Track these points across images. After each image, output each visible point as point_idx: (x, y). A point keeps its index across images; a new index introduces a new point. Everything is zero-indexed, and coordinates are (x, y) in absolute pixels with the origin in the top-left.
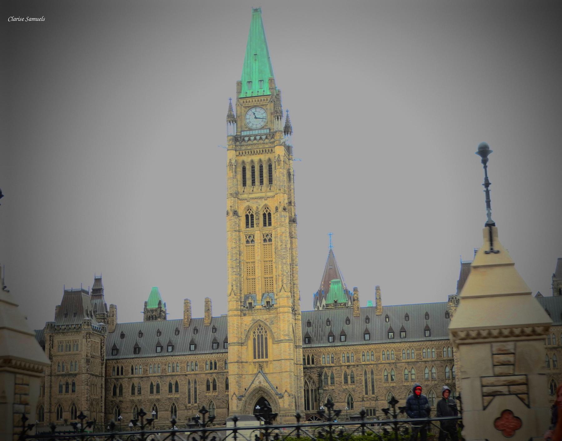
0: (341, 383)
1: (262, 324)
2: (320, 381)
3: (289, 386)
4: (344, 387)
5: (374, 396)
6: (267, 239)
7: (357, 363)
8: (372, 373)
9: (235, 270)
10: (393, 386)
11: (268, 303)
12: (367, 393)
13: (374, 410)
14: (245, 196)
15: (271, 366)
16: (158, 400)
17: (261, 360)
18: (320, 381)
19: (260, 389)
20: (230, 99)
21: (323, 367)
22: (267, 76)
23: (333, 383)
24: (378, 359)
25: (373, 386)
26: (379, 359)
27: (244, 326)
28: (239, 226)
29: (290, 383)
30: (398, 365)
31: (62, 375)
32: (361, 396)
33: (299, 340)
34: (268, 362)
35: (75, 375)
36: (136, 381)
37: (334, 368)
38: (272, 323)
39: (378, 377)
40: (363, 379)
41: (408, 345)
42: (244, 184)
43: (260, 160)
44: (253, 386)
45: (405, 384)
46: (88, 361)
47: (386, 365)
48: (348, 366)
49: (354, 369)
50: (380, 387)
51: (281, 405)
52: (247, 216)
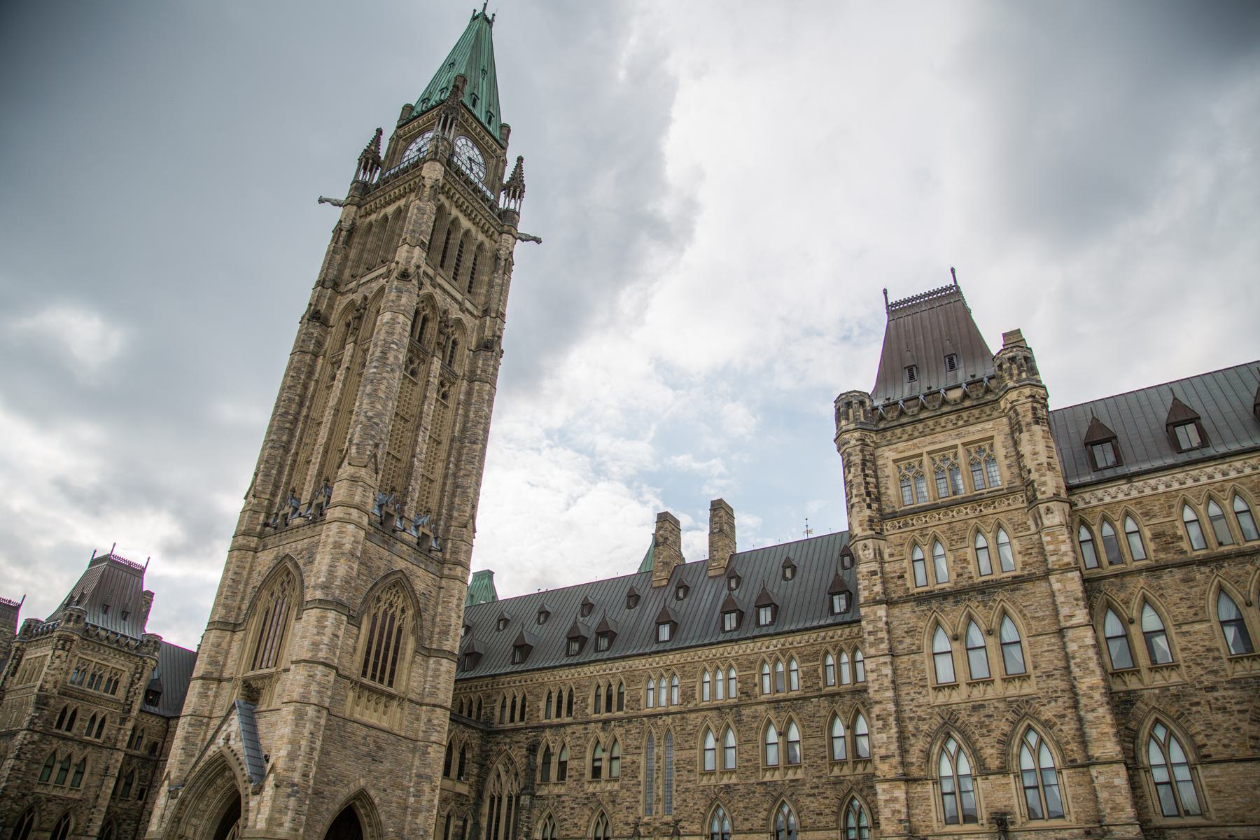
0: (582, 775)
1: (289, 565)
2: (531, 770)
3: (283, 753)
4: (590, 789)
5: (669, 818)
7: (631, 713)
9: (274, 437)
10: (727, 786)
12: (648, 810)
15: (278, 688)
18: (531, 770)
20: (380, 132)
21: (541, 728)
23: (562, 775)
26: (693, 696)
27: (255, 575)
28: (319, 344)
29: (294, 743)
30: (746, 712)
32: (631, 819)
33: (445, 633)
34: (270, 676)
37: (569, 730)
39: (685, 754)
46: (42, 702)
47: (709, 713)
48: (606, 722)
49: (618, 732)
50: (687, 790)
51: (252, 816)
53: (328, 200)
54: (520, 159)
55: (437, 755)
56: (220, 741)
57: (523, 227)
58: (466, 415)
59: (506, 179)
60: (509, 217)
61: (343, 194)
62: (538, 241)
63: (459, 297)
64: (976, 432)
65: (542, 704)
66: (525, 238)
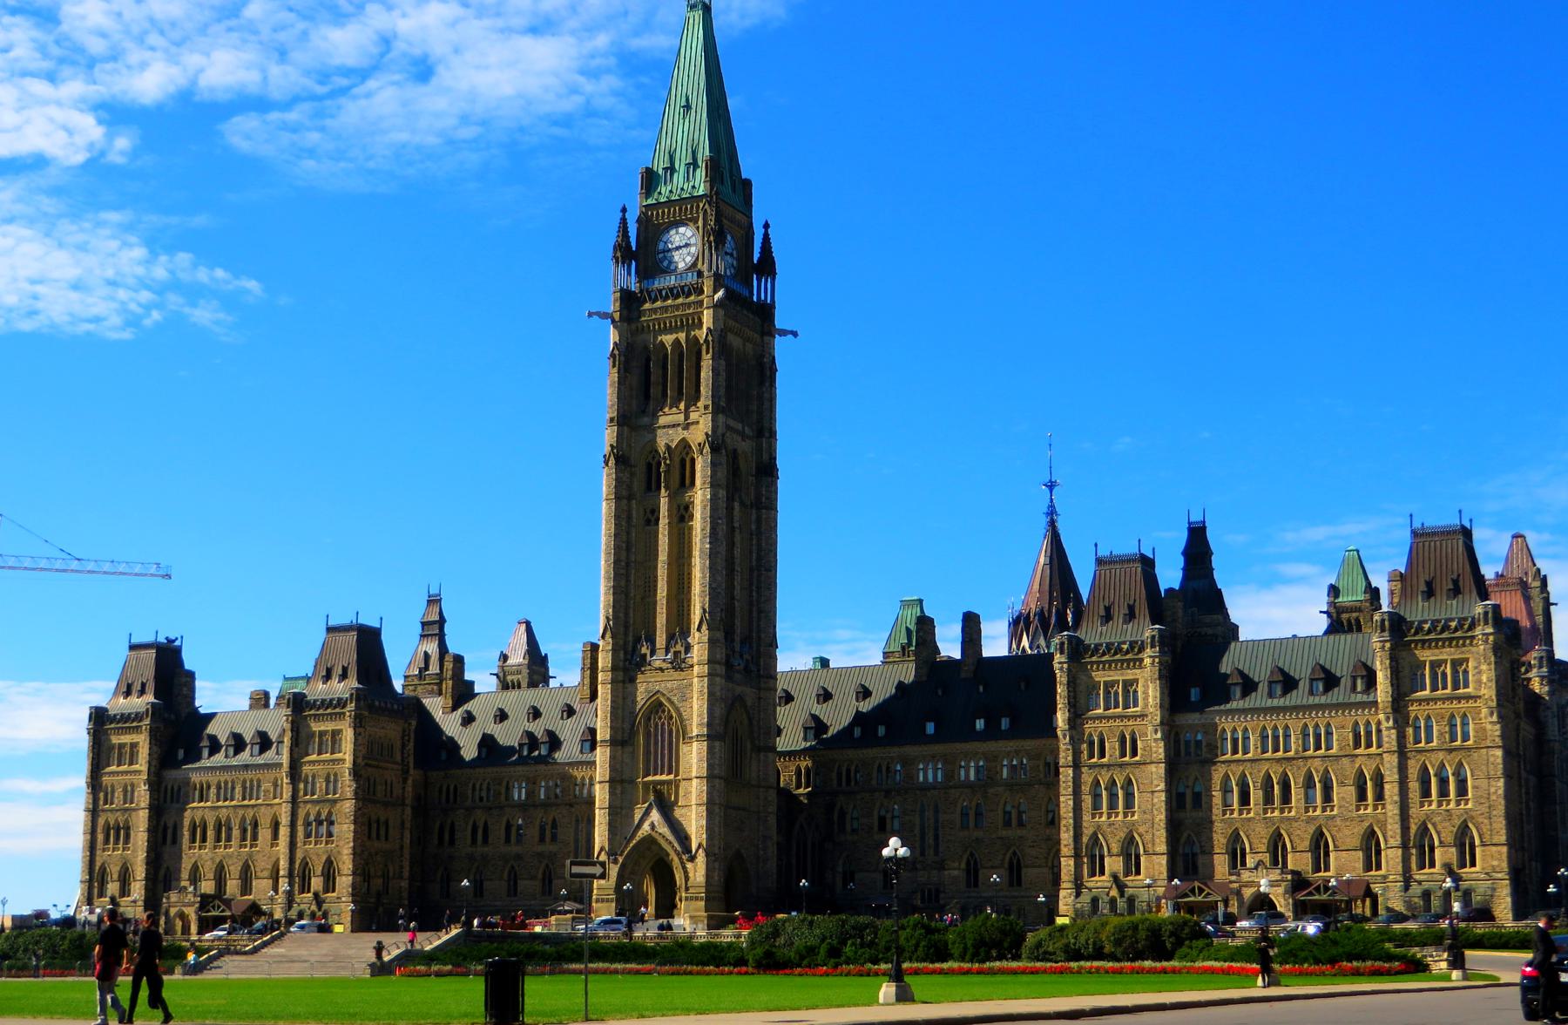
6: (682, 514)
8: (936, 811)
11: (676, 653)
13: (938, 891)
14: (646, 420)
16: (518, 857)
17: (658, 778)
19: (650, 841)
20: (624, 210)
22: (704, 152)
24: (950, 775)
25: (936, 837)
28: (630, 487)
30: (991, 791)
31: (312, 802)
34: (669, 783)
35: (335, 801)
36: (480, 817)
38: (684, 698)
40: (917, 821)
41: (1011, 745)
42: (647, 396)
43: (677, 341)
44: (641, 834)
45: (1004, 833)
46: (356, 772)
52: (649, 466)
53: (598, 314)
54: (766, 226)
55: (772, 820)
56: (646, 827)
57: (779, 322)
58: (759, 545)
59: (756, 256)
60: (766, 312)
61: (612, 305)
62: (795, 334)
63: (740, 426)
64: (1130, 674)
65: (834, 775)
66: (784, 333)
